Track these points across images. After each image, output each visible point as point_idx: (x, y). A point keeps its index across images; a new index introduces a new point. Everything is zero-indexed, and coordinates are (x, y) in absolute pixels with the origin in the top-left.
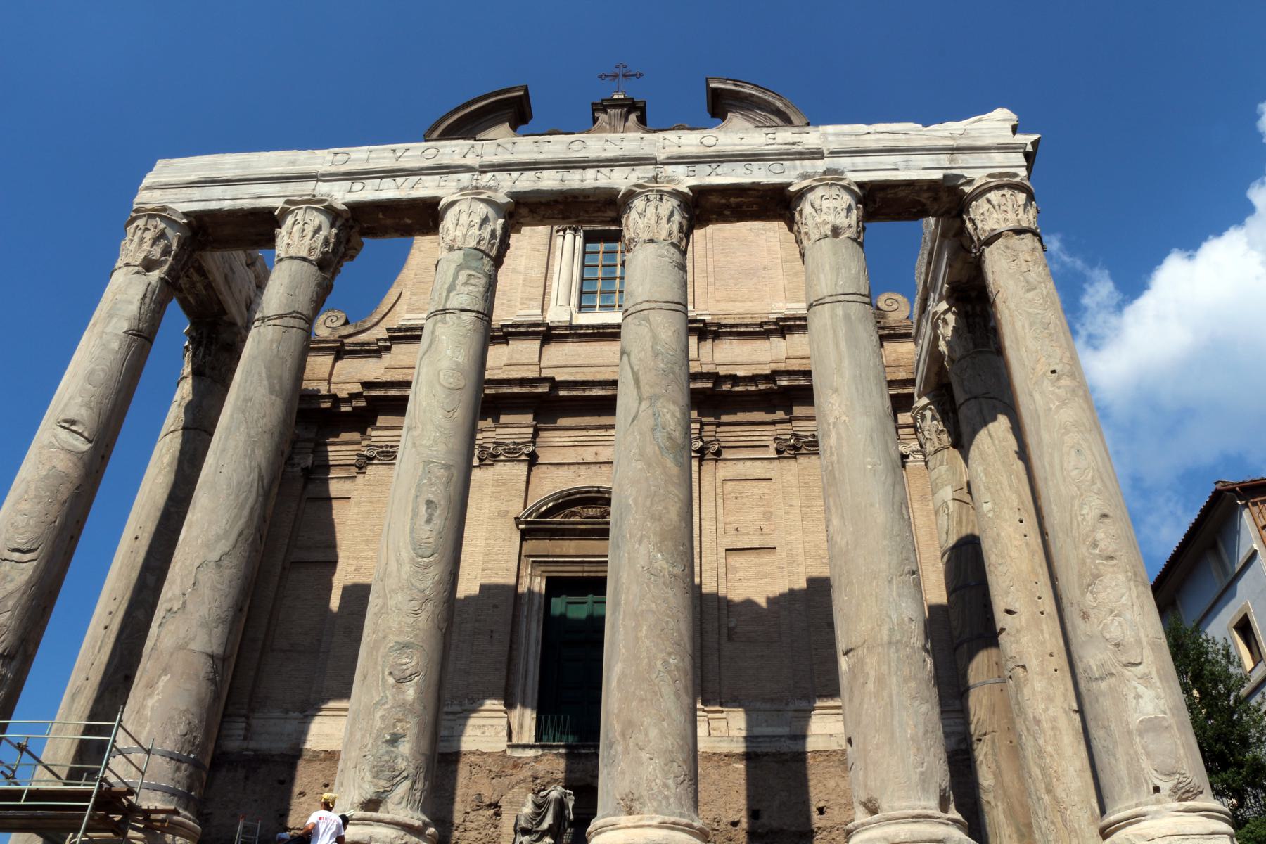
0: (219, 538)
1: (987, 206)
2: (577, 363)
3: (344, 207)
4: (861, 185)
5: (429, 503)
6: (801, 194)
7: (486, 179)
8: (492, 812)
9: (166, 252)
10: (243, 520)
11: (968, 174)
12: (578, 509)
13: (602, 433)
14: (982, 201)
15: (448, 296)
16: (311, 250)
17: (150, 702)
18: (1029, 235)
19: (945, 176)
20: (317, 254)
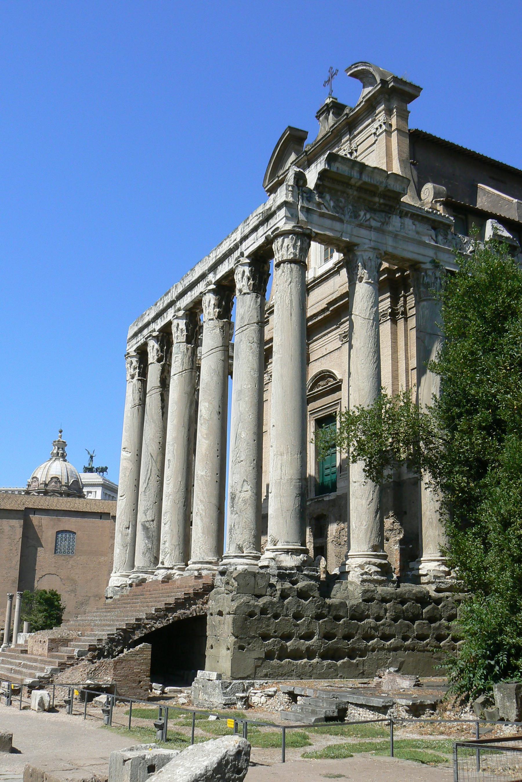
2: (319, 299)
3: (158, 333)
5: (169, 460)
9: (135, 369)
10: (149, 474)
12: (320, 383)
13: (326, 337)
16: (154, 357)
18: (282, 265)
19: (266, 238)
20: (156, 357)
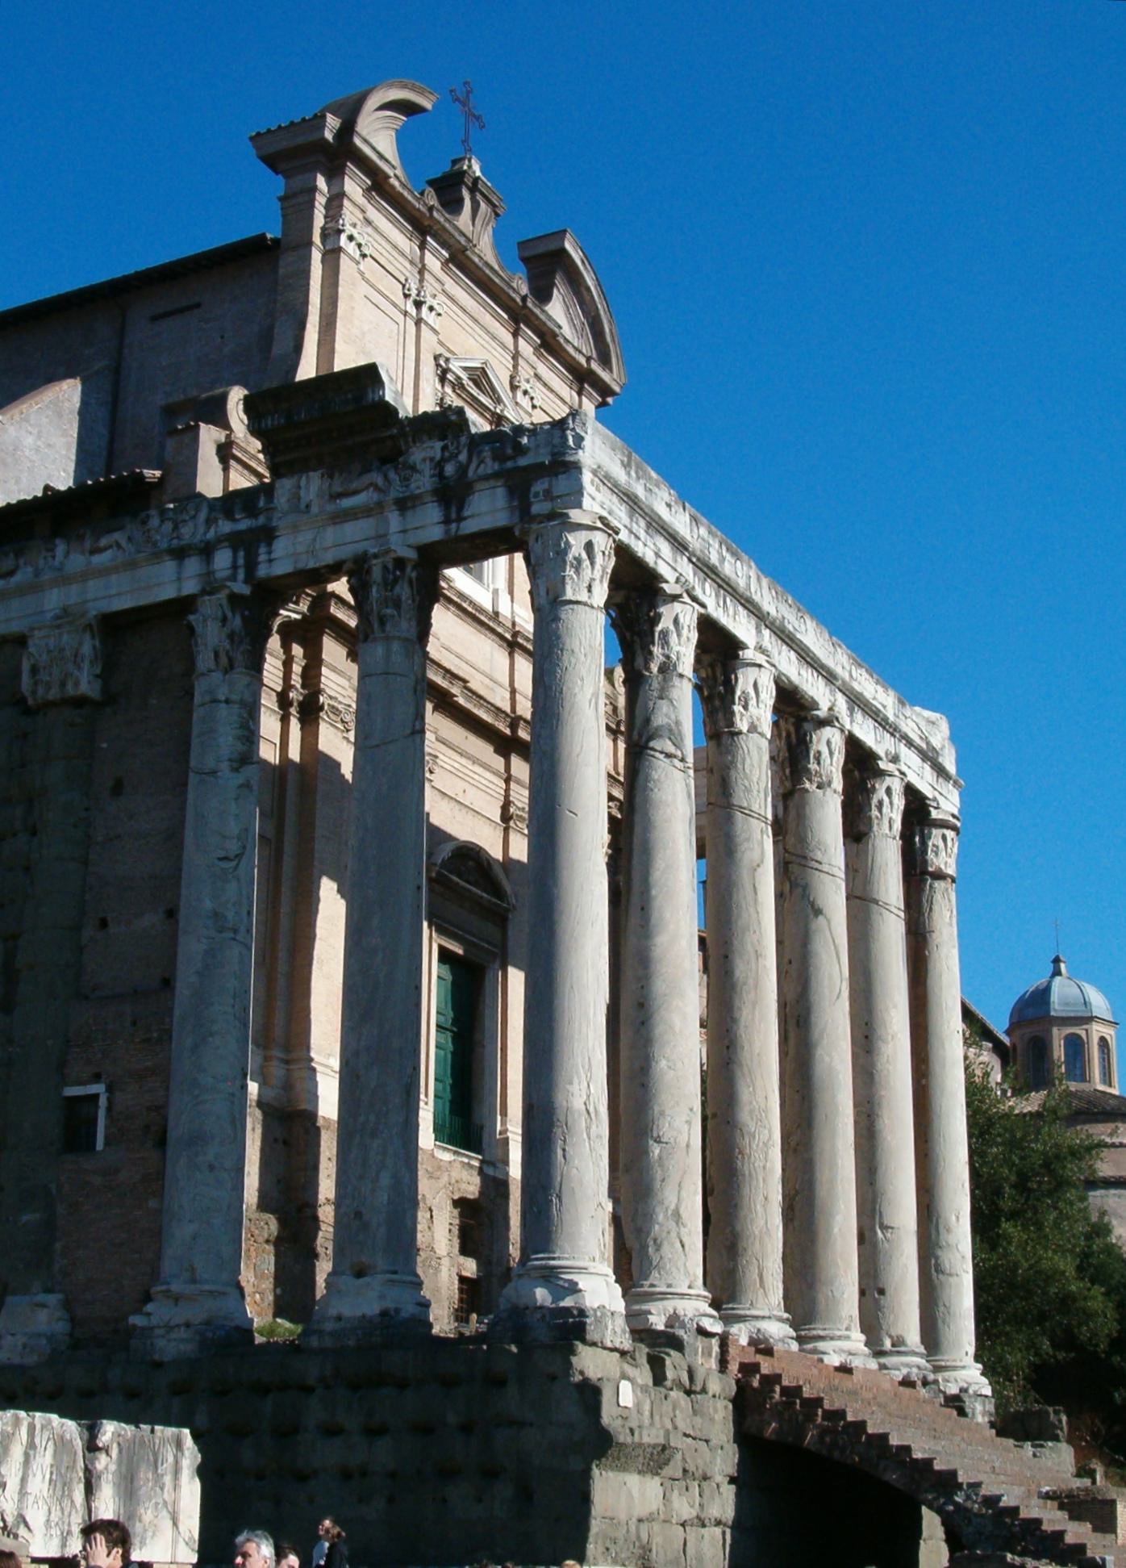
1: (941, 844)
6: (882, 774)
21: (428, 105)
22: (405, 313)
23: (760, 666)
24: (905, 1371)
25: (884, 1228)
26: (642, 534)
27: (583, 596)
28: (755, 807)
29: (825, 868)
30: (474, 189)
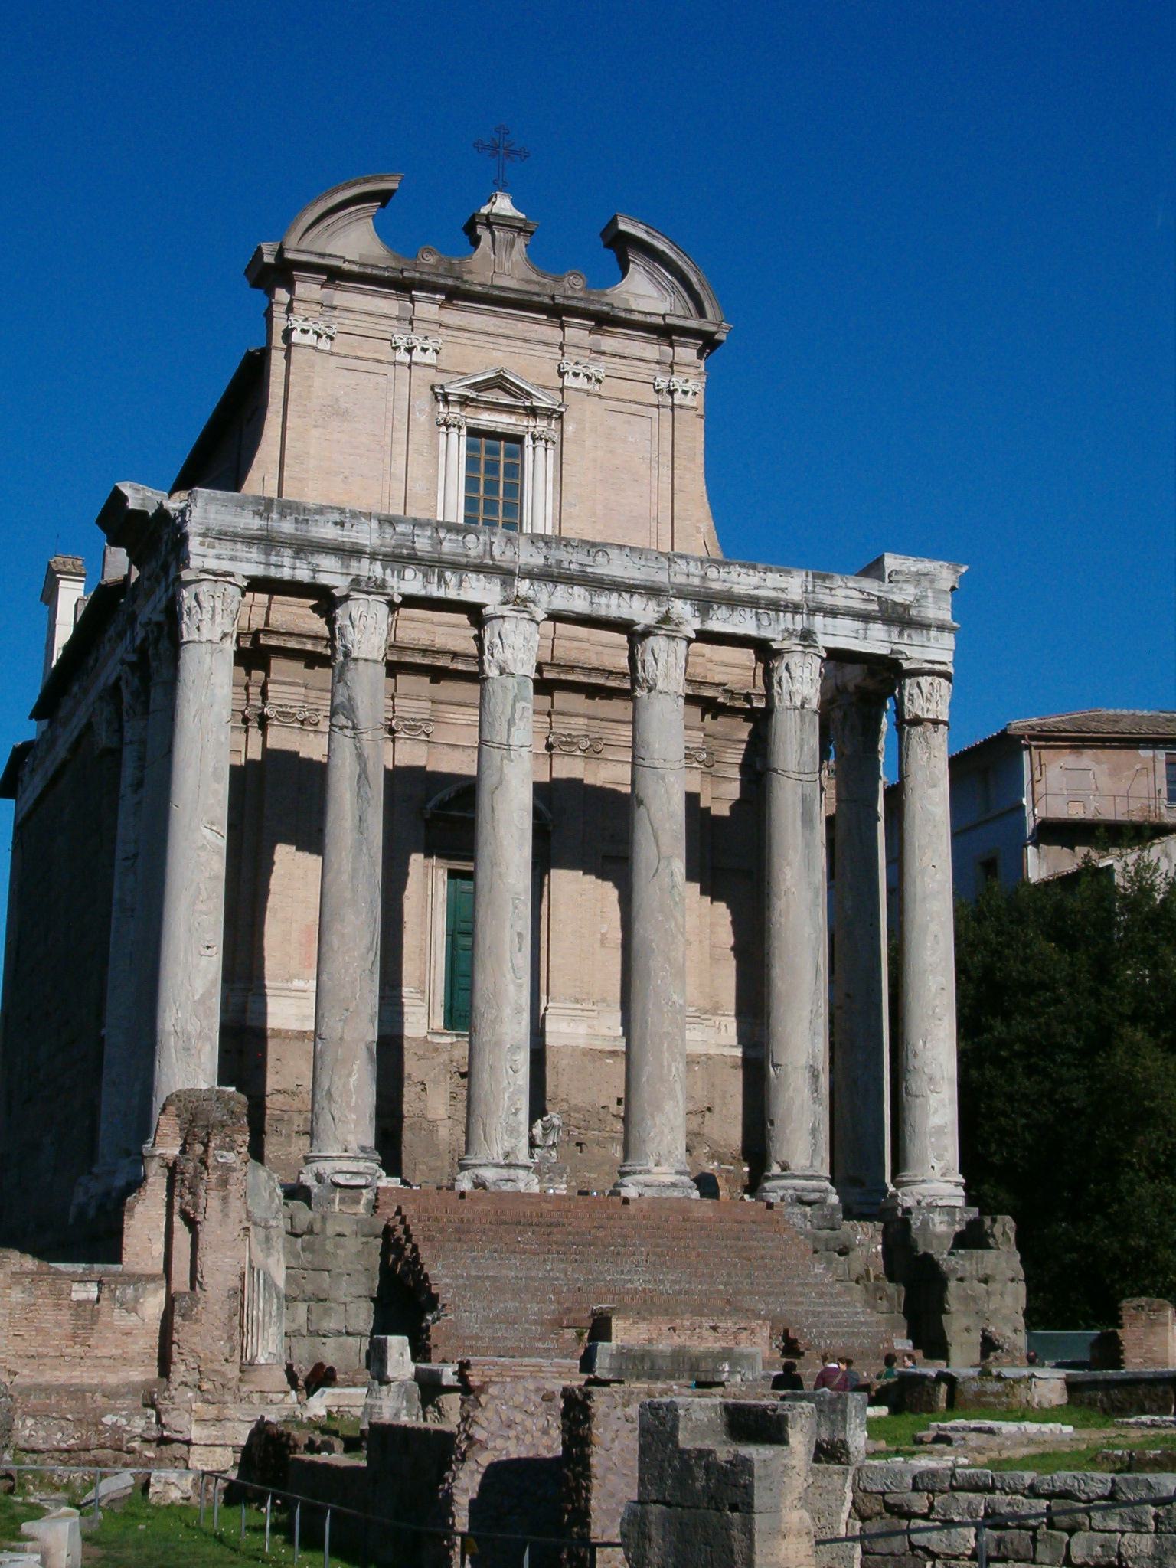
0: (370, 949)
1: (916, 691)
4: (827, 649)
5: (519, 934)
7: (523, 587)
8: (419, 1088)
11: (908, 651)
14: (914, 680)
15: (509, 730)
17: (353, 1080)
18: (941, 726)
21: (393, 185)
22: (394, 364)
23: (503, 617)
24: (781, 1193)
25: (775, 1066)
26: (287, 561)
27: (195, 637)
28: (498, 739)
29: (647, 763)
30: (489, 225)
